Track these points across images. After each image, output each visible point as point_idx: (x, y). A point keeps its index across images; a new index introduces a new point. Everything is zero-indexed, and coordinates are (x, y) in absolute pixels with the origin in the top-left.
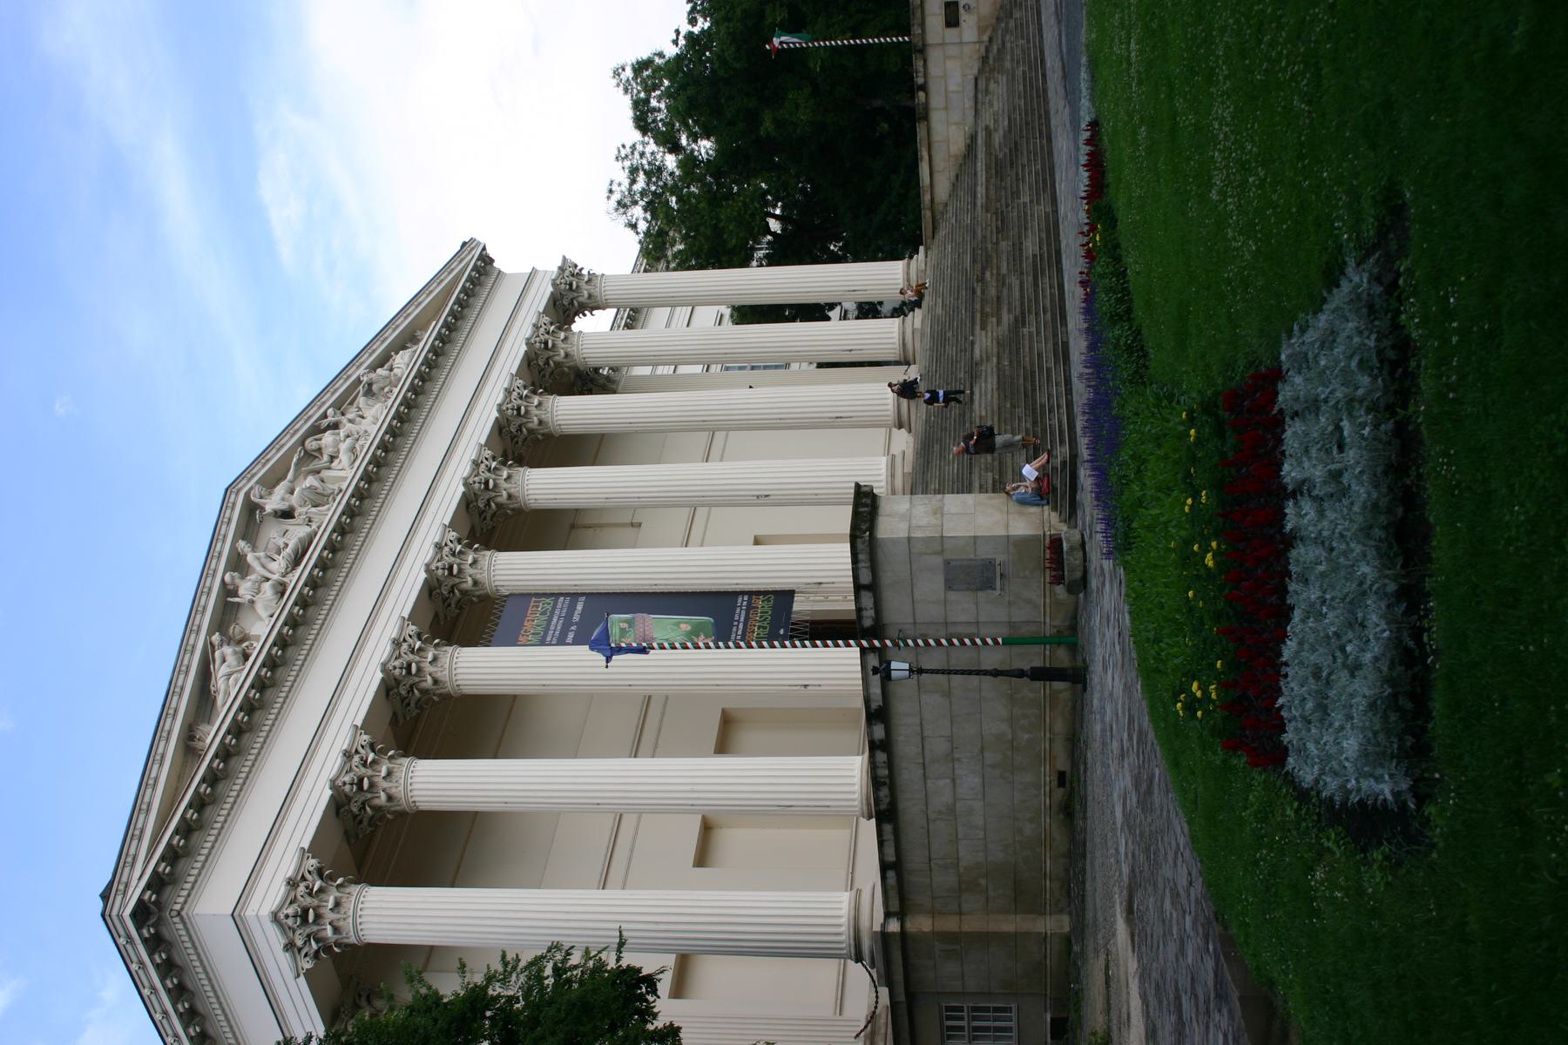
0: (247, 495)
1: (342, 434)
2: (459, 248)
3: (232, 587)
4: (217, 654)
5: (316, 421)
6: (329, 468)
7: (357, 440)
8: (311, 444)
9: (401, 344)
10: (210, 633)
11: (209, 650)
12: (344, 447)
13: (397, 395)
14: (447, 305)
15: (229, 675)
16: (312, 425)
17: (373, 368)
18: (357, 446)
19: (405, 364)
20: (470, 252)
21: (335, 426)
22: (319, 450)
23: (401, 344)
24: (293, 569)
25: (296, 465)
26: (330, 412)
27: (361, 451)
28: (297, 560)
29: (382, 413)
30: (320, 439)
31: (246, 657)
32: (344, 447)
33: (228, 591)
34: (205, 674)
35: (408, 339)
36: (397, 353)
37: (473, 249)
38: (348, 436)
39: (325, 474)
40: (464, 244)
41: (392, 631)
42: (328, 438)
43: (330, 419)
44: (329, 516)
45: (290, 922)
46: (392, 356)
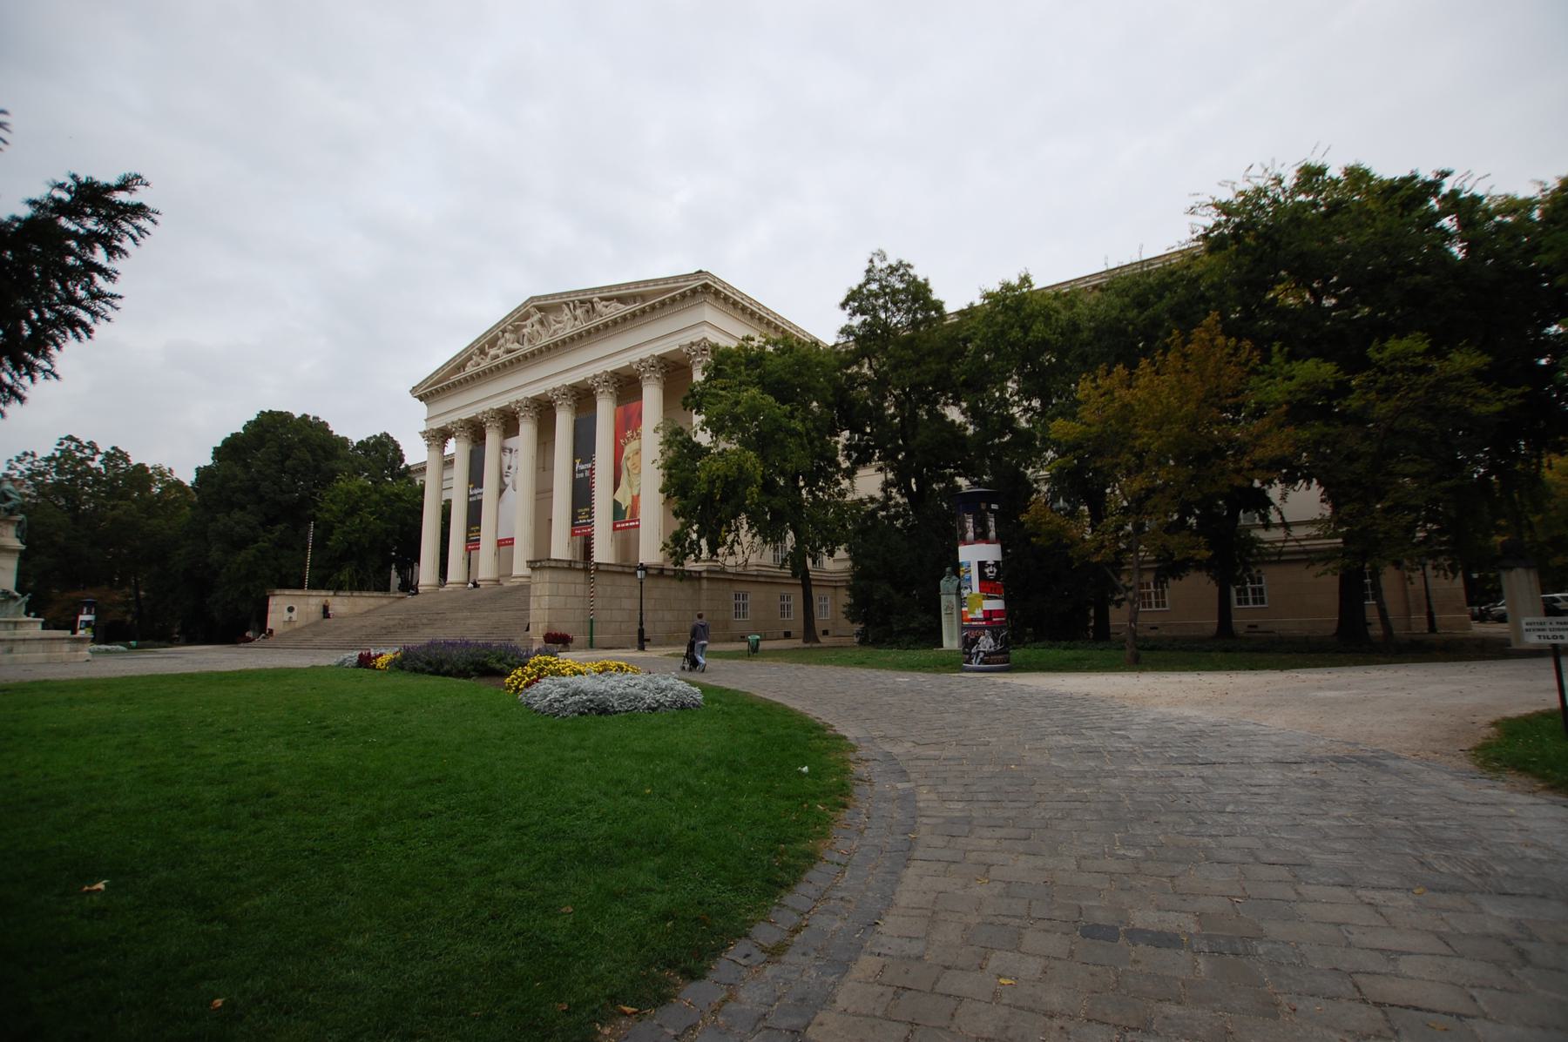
2: (693, 272)
5: (571, 301)
9: (621, 299)
11: (473, 354)
13: (597, 321)
17: (602, 299)
19: (616, 310)
23: (621, 299)
28: (509, 351)
31: (479, 365)
34: (470, 358)
35: (633, 298)
40: (700, 272)
41: (520, 397)
44: (527, 348)
45: (703, 344)
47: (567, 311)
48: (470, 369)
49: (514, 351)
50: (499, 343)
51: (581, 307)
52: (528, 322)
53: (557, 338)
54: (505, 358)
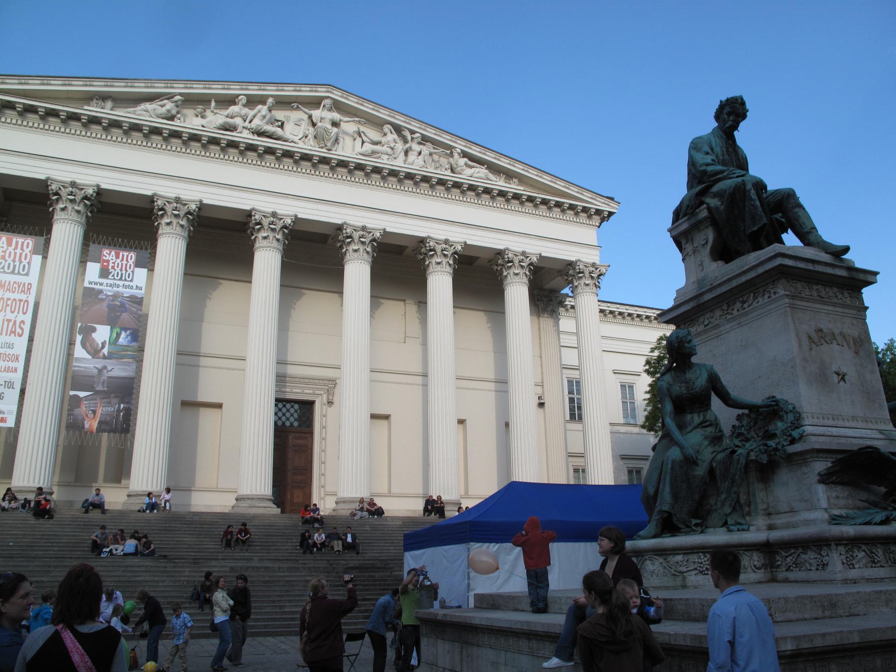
0: (328, 97)
1: (392, 145)
3: (237, 101)
4: (166, 101)
6: (363, 142)
7: (388, 154)
8: (387, 128)
10: (180, 94)
11: (170, 97)
12: (385, 149)
13: (446, 174)
14: (538, 194)
15: (147, 111)
16: (401, 126)
17: (465, 154)
18: (380, 155)
19: (478, 175)
20: (605, 203)
21: (405, 141)
22: (385, 134)
24: (253, 133)
25: (355, 120)
26: (417, 135)
27: (375, 158)
28: (261, 133)
29: (417, 166)
30: (391, 133)
31: (172, 118)
32: (385, 149)
33: (231, 101)
35: (509, 175)
36: (487, 168)
37: (609, 205)
38: (392, 149)
39: (359, 141)
40: (612, 199)
42: (392, 137)
43: (409, 138)
46: (484, 166)
47: (395, 136)
48: (146, 114)
49: (270, 137)
50: (233, 109)
51: (420, 143)
52: (317, 114)
53: (371, 162)
54: (244, 136)
